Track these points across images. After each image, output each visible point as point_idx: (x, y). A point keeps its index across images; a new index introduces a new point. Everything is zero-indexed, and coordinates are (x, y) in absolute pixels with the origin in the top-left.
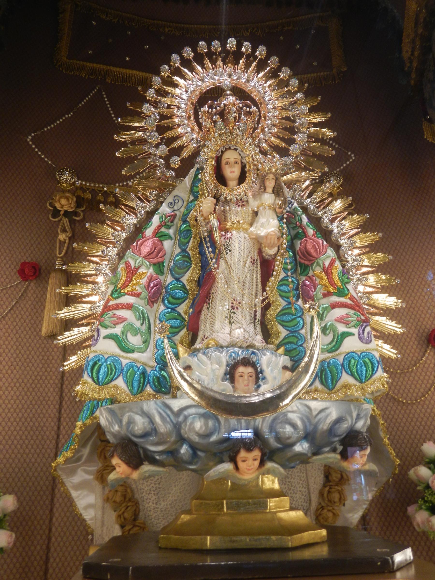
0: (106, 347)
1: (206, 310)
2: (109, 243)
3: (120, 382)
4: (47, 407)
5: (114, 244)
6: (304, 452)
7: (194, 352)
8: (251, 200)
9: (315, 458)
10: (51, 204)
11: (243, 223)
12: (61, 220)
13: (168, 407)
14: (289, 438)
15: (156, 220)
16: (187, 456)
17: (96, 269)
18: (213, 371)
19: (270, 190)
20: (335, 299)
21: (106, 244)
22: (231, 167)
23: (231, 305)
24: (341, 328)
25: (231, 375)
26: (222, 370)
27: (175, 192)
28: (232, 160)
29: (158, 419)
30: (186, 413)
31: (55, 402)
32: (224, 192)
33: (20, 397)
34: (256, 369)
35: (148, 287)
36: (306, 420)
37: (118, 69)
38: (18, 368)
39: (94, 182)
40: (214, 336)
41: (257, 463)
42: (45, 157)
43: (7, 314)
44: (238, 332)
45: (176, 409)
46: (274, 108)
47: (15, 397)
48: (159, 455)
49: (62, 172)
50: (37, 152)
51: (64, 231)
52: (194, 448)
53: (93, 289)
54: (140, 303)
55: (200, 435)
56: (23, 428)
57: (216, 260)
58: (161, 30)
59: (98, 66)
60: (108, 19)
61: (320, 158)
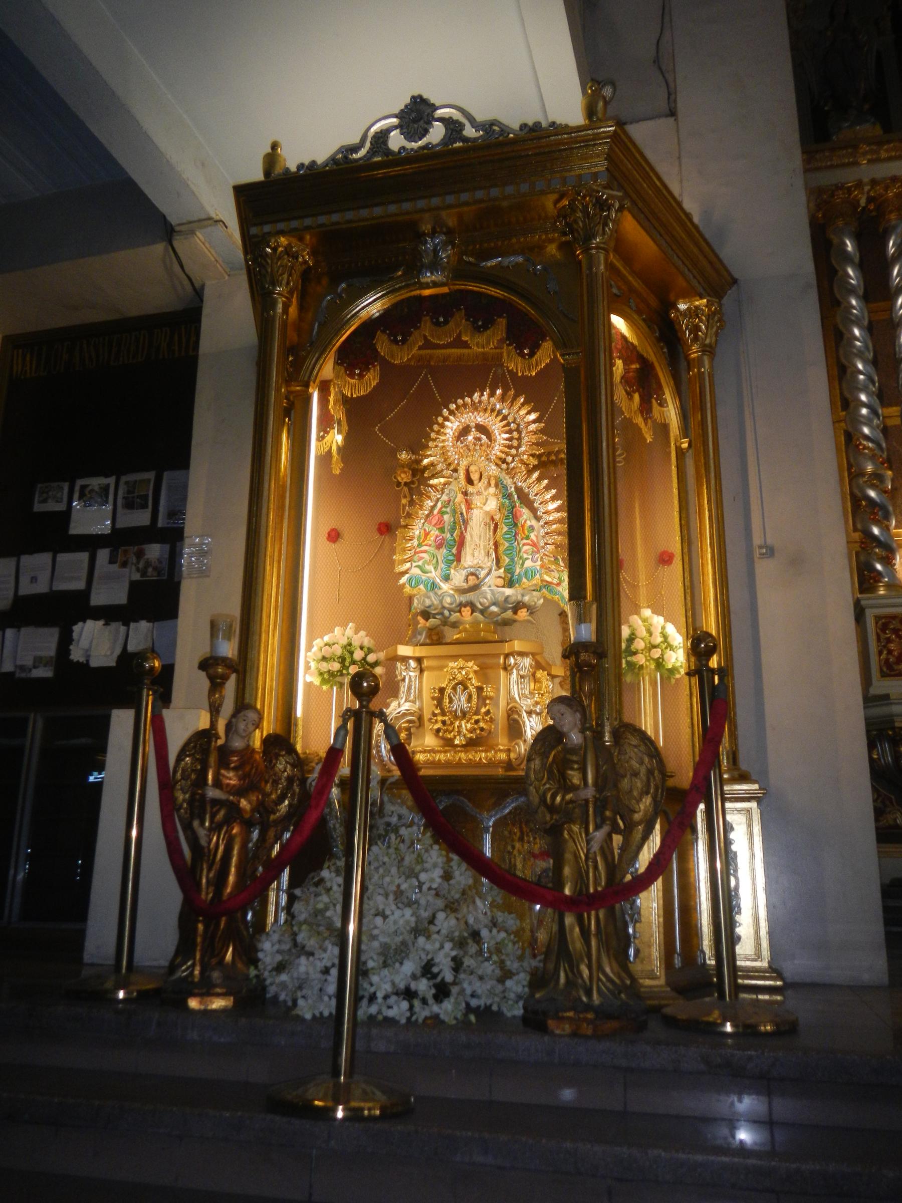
0: (416, 571)
3: (422, 587)
15: (439, 505)
20: (525, 541)
24: (525, 556)
25: (467, 580)
26: (463, 577)
27: (450, 487)
35: (435, 541)
51: (405, 497)
54: (432, 550)
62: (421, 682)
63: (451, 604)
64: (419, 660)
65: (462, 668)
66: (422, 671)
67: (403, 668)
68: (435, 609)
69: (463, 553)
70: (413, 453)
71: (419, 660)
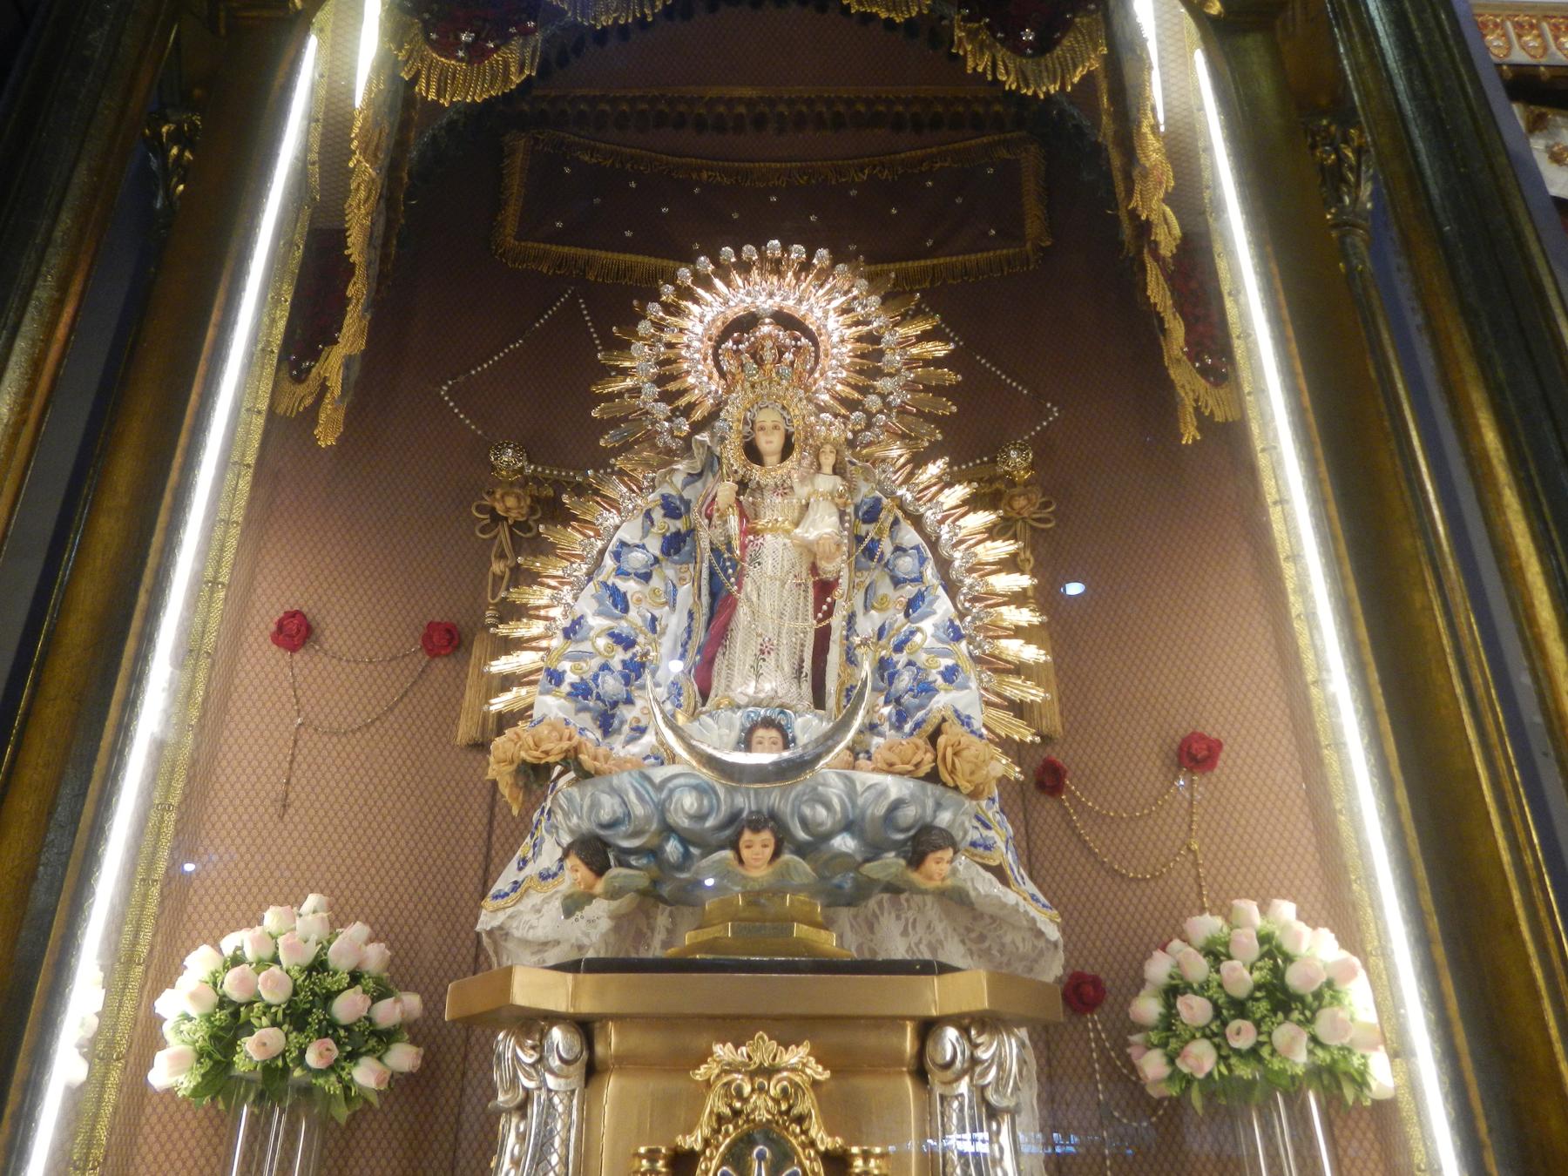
4: (462, 873)
5: (582, 558)
7: (694, 715)
8: (796, 487)
9: (868, 865)
10: (480, 509)
13: (648, 779)
14: (821, 824)
17: (553, 598)
18: (720, 737)
19: (828, 469)
21: (570, 557)
26: (734, 735)
28: (769, 424)
29: (632, 797)
30: (671, 785)
31: (476, 865)
34: (784, 735)
37: (610, 255)
39: (560, 467)
41: (769, 851)
43: (396, 704)
44: (768, 686)
45: (657, 780)
46: (842, 341)
49: (500, 450)
50: (457, 415)
51: (502, 556)
52: (685, 841)
53: (547, 629)
56: (420, 907)
59: (573, 250)
62: (588, 1122)
63: (701, 817)
64: (585, 1027)
65: (769, 1072)
66: (592, 1071)
67: (528, 1058)
68: (636, 834)
69: (720, 663)
70: (530, 462)
71: (585, 1027)
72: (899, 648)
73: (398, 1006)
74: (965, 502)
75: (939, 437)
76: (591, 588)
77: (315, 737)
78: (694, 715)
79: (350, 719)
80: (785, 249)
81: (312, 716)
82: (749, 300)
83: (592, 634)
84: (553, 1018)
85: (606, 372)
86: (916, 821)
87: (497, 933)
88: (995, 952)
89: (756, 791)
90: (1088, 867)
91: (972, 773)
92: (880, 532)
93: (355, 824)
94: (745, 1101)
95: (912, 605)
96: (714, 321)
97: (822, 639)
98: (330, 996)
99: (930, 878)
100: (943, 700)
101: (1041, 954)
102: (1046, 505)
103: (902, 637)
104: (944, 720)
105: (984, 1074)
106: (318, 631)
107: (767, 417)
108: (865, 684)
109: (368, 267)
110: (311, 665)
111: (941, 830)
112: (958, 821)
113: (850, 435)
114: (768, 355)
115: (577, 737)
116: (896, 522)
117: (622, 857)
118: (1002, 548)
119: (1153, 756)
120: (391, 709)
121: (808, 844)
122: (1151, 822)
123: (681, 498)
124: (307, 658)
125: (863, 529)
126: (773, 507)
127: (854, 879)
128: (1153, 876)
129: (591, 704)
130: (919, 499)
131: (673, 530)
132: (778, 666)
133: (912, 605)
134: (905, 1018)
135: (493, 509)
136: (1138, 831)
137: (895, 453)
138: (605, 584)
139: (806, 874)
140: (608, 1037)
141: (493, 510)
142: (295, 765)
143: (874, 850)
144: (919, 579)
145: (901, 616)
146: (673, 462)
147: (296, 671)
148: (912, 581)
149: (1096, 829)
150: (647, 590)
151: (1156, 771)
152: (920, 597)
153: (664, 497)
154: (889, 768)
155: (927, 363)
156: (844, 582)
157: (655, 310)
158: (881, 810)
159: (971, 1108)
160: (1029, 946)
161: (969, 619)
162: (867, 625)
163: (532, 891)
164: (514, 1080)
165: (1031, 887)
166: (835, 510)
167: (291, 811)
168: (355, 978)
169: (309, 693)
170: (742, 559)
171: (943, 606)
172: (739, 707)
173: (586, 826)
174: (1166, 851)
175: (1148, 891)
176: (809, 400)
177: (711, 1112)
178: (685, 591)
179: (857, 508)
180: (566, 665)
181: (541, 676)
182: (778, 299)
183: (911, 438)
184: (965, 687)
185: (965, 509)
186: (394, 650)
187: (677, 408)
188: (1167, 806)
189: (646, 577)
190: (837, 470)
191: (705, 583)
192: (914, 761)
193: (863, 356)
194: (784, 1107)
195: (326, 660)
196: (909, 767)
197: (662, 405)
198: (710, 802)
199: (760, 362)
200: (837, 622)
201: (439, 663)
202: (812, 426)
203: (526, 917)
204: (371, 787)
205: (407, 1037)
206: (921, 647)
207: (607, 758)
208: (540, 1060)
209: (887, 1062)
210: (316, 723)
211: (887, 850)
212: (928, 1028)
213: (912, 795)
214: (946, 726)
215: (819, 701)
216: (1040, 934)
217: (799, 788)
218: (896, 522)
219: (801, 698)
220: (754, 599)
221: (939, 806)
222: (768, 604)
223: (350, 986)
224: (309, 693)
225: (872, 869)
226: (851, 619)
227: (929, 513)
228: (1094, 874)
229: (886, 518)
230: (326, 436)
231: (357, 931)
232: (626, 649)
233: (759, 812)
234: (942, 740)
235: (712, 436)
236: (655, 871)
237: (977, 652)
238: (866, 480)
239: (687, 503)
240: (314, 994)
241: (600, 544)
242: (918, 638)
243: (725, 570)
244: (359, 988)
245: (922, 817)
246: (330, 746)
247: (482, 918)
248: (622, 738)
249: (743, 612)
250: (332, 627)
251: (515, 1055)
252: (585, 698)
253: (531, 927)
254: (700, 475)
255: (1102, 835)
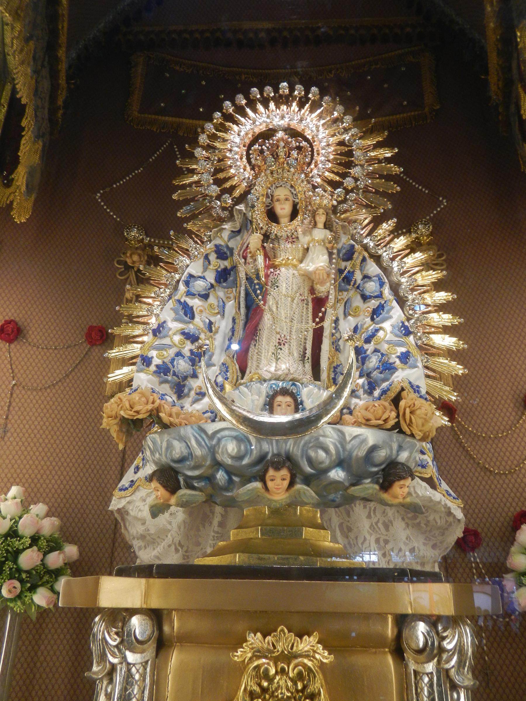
1: (253, 347)
2: (162, 284)
4: (108, 468)
5: (166, 285)
6: (341, 480)
7: (236, 385)
8: (301, 236)
9: (353, 488)
10: (119, 263)
11: (292, 260)
12: (128, 278)
13: (203, 430)
14: (321, 463)
16: (223, 482)
18: (253, 401)
19: (321, 225)
21: (158, 285)
22: (281, 204)
23: (278, 341)
25: (270, 406)
26: (262, 400)
28: (282, 197)
29: (193, 443)
30: (219, 435)
31: (117, 464)
32: (275, 229)
33: (82, 457)
34: (295, 400)
36: (339, 446)
37: (191, 121)
38: (80, 427)
40: (260, 372)
41: (286, 483)
42: (114, 214)
43: (71, 372)
45: (210, 432)
46: (328, 145)
47: (77, 456)
48: (198, 482)
49: (130, 229)
52: (229, 472)
53: (144, 330)
55: (232, 458)
57: (263, 297)
58: (237, 78)
60: (182, 69)
61: (384, 194)
63: (239, 458)
64: (156, 616)
66: (162, 644)
68: (195, 467)
70: (147, 236)
71: (156, 616)
72: (368, 341)
73: (61, 556)
74: (407, 247)
75: (390, 207)
76: (170, 304)
77: (23, 392)
78: (236, 385)
79: (43, 382)
80: (292, 89)
81: (21, 379)
82: (268, 121)
83: (171, 333)
84: (132, 612)
85: (181, 173)
86: (386, 459)
87: (123, 510)
88: (423, 525)
89: (277, 441)
90: (470, 466)
91: (423, 425)
92: (354, 266)
93: (47, 441)
94: (271, 680)
95: (375, 313)
96: (247, 134)
97: (318, 335)
98: (17, 553)
99: (396, 497)
100: (401, 376)
101: (450, 525)
102: (440, 256)
103: (370, 333)
104: (403, 389)
105: (448, 661)
106: (25, 332)
107: (281, 193)
108: (351, 366)
109: (36, 109)
110: (21, 351)
111: (403, 464)
112: (413, 457)
113: (335, 203)
114: (282, 154)
115: (158, 401)
116: (364, 260)
117: (188, 481)
118: (432, 276)
119: (508, 401)
120: (67, 376)
121: (312, 475)
122: (507, 440)
123: (227, 247)
124: (18, 347)
125: (343, 264)
126: (286, 250)
127: (342, 495)
128: (510, 472)
129: (170, 378)
130: (378, 245)
131: (222, 267)
132: (290, 353)
133: (375, 313)
134: (387, 614)
135: (126, 262)
136: (500, 445)
137: (362, 217)
138: (179, 301)
139: (313, 498)
140: (172, 622)
141: (125, 263)
142: (11, 408)
143: (356, 479)
144: (380, 296)
145: (368, 320)
146: (221, 225)
147: (12, 354)
148: (376, 297)
149: (474, 443)
150: (206, 305)
151: (510, 410)
152: (381, 307)
153: (216, 246)
154: (367, 423)
155: (380, 161)
156: (332, 297)
157: (209, 127)
158: (362, 452)
159: (439, 685)
160: (443, 521)
161: (412, 321)
162: (346, 327)
163: (141, 488)
164: (103, 657)
165: (444, 486)
166: (326, 251)
167: (9, 434)
168: (35, 540)
169: (20, 367)
170: (266, 284)
171: (397, 313)
172: (265, 381)
173: (164, 460)
174: (517, 458)
175: (507, 481)
176: (309, 182)
177: (245, 689)
178: (230, 305)
179: (339, 251)
180: (153, 353)
181: (139, 360)
182: (287, 120)
183: (372, 207)
184: (415, 366)
185: (407, 251)
186: (69, 342)
187: (225, 189)
188: (517, 431)
189: (205, 297)
190: (328, 226)
191: (242, 300)
192: (384, 418)
193: (341, 154)
194: (300, 686)
195: (30, 348)
196: (381, 422)
197: (214, 187)
198: (246, 447)
199: (276, 156)
200: (327, 324)
201: (96, 350)
202: (310, 197)
203: (137, 504)
204: (56, 420)
205: (69, 571)
206: (383, 340)
207: (178, 415)
208: (122, 642)
209: (375, 643)
210: (24, 384)
211: (366, 478)
212: (403, 621)
213: (384, 442)
214: (404, 394)
215: (316, 374)
216: (449, 513)
217: (307, 438)
218: (364, 260)
219: (305, 373)
220: (274, 309)
221: (401, 448)
222: (283, 313)
223: (31, 546)
224: (20, 367)
225: (354, 490)
226: (336, 321)
227: (385, 254)
228: (473, 470)
229: (357, 258)
230: (20, 217)
231: (39, 509)
232: (192, 342)
233: (278, 455)
234: (402, 403)
235: (246, 207)
236: (209, 490)
237: (419, 343)
238: (345, 233)
239: (231, 250)
240: (7, 551)
241: (177, 276)
242: (381, 334)
243: (255, 291)
244: (35, 548)
245: (390, 456)
246: (32, 397)
247: (113, 502)
248: (190, 400)
249: (267, 319)
250: (33, 329)
251: (104, 638)
252: (165, 375)
253: (140, 510)
254: (239, 232)
255: (477, 447)
